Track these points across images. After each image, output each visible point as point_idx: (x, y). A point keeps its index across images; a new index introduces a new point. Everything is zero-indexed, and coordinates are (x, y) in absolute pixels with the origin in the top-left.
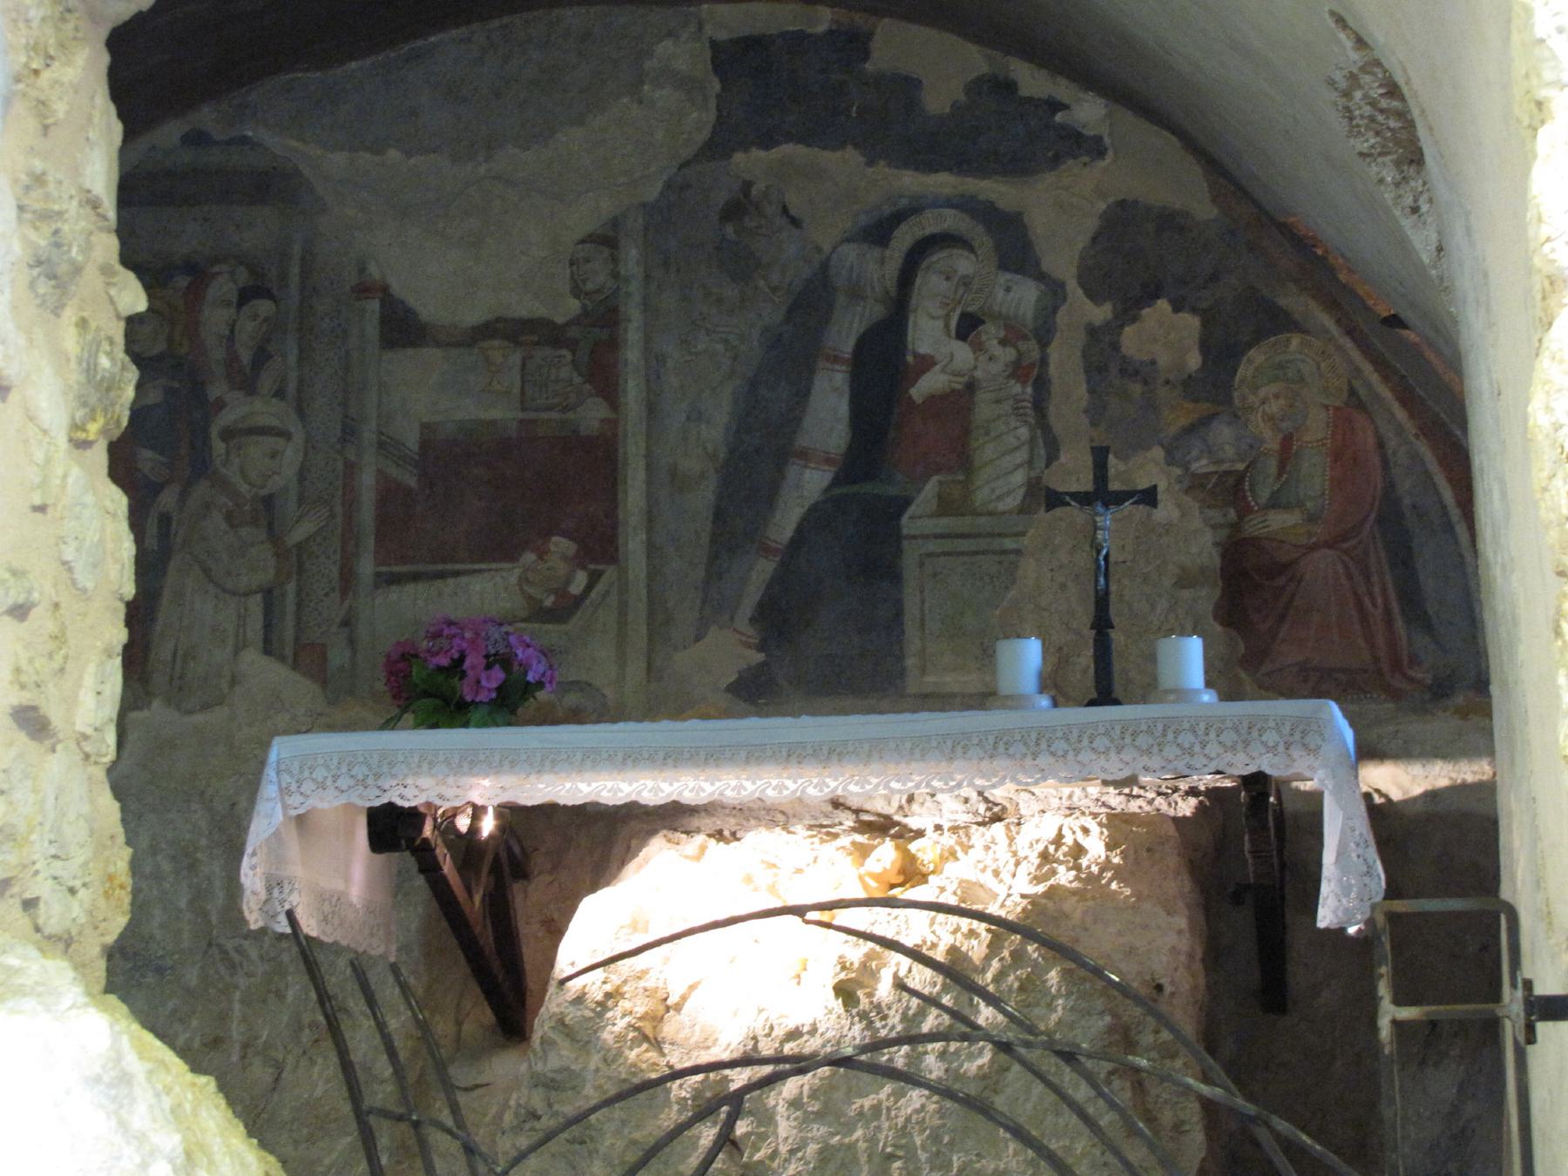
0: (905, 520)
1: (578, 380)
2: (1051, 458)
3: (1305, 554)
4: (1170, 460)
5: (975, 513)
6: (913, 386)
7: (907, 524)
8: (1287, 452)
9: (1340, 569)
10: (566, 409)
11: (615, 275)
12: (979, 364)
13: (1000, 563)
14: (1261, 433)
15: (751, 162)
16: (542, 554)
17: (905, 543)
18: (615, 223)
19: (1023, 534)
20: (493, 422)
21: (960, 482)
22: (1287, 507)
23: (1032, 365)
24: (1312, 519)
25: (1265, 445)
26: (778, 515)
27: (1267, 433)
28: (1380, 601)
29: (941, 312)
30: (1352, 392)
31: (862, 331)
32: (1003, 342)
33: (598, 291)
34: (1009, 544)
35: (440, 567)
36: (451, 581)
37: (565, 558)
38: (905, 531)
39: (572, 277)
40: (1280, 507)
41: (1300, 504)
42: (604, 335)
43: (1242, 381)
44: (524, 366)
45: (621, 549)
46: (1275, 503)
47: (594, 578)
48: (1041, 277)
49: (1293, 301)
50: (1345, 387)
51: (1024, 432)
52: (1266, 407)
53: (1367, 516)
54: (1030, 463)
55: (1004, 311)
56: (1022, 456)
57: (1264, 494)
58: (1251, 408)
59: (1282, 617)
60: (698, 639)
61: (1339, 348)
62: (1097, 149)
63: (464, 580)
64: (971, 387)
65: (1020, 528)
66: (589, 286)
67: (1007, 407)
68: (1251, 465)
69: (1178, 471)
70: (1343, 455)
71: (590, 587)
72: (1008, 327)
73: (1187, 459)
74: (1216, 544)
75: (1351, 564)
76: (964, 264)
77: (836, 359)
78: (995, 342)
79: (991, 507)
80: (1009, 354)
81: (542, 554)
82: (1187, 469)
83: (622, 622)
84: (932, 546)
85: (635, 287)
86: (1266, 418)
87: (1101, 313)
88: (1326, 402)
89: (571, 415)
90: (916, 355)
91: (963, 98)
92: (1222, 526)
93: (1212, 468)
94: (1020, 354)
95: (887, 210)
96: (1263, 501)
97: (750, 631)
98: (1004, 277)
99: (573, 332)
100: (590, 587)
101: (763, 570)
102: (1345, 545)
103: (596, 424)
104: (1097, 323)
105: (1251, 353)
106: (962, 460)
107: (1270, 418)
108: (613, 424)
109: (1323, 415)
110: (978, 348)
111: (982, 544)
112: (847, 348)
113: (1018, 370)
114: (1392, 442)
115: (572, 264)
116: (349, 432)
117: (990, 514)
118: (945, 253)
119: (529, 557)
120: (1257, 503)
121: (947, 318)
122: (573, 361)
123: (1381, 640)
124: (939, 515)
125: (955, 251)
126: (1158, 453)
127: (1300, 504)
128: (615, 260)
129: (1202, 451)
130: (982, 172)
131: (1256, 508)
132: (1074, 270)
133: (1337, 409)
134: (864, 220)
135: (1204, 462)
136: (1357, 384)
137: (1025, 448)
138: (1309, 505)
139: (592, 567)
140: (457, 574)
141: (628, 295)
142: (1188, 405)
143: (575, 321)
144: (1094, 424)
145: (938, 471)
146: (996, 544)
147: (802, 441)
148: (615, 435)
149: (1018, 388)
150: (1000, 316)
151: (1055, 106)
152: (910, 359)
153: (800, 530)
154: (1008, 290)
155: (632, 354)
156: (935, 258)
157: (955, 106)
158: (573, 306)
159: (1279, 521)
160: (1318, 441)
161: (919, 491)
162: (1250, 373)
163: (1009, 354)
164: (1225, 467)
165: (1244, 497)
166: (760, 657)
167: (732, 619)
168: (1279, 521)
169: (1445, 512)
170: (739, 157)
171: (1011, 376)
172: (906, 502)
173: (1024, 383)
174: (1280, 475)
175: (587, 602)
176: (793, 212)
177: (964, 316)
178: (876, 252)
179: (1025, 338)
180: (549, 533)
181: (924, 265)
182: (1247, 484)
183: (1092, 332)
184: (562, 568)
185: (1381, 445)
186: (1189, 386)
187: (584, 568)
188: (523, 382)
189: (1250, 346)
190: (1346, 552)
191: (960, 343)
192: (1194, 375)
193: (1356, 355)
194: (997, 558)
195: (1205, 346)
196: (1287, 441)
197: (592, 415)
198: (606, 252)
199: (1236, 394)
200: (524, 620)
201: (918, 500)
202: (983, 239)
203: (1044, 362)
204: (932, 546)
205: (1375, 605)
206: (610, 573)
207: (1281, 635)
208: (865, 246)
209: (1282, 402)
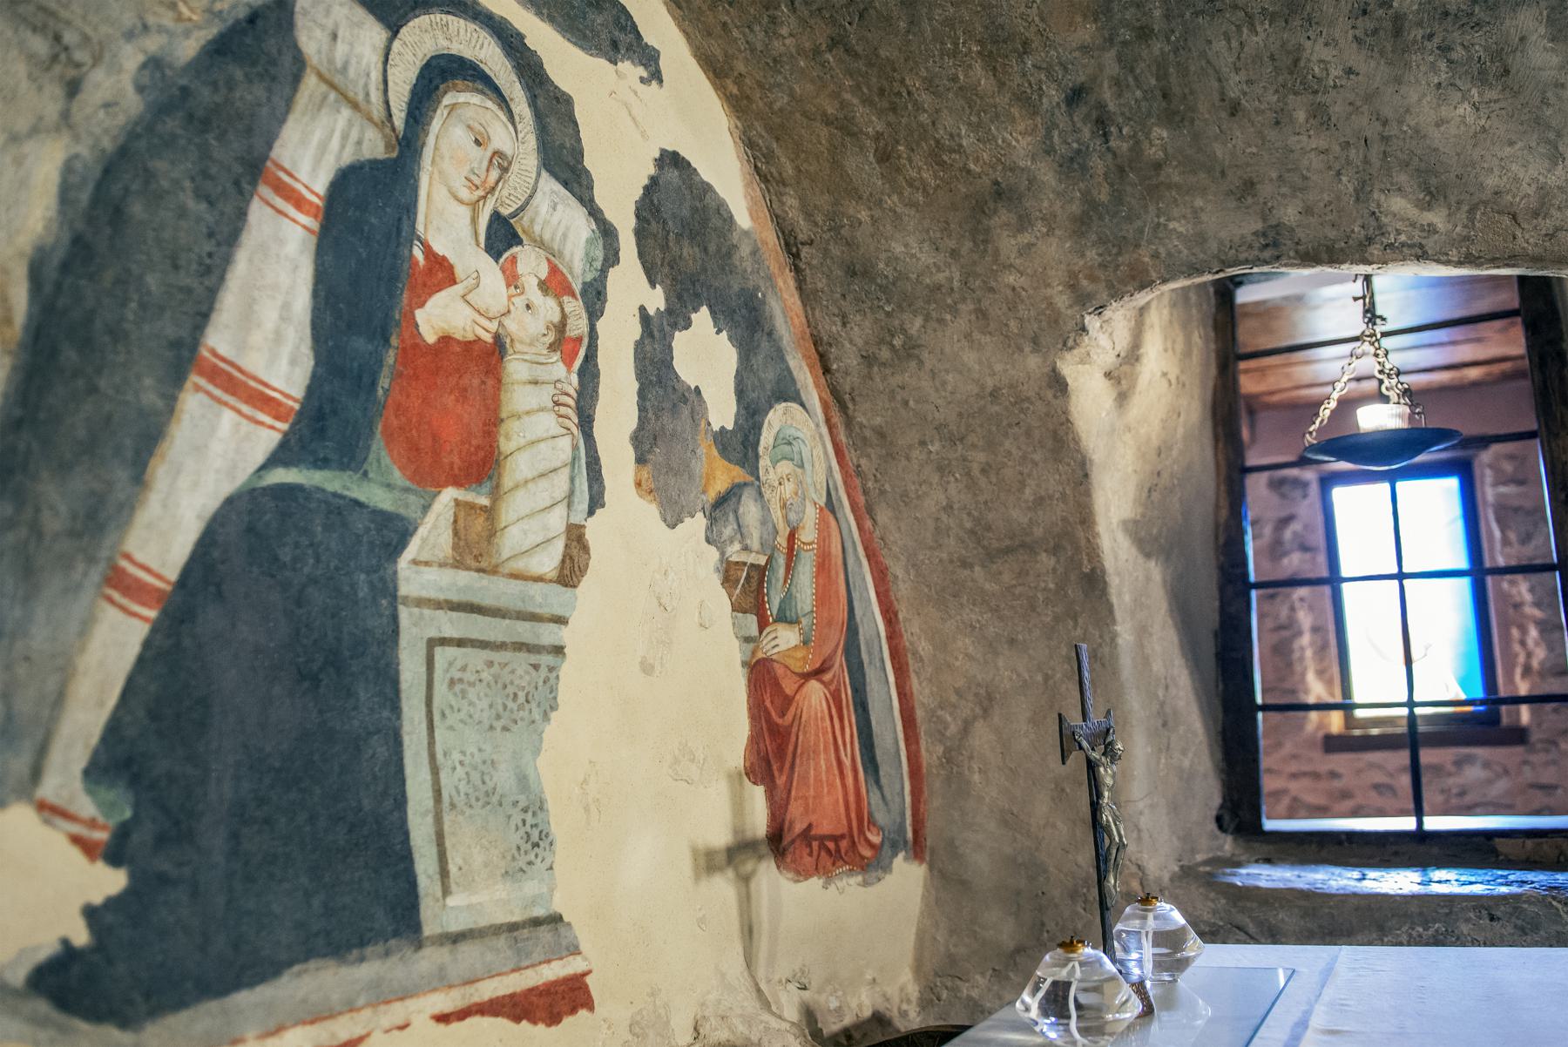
0: (403, 562)
5: (493, 571)
12: (512, 308)
13: (536, 667)
17: (404, 614)
19: (561, 621)
21: (483, 509)
23: (579, 339)
29: (465, 194)
38: (403, 590)
51: (565, 444)
53: (840, 640)
55: (547, 237)
56: (561, 483)
65: (558, 611)
72: (554, 270)
79: (519, 565)
84: (450, 625)
88: (816, 500)
97: (86, 807)
111: (524, 631)
112: (315, 180)
113: (561, 341)
117: (515, 576)
124: (458, 564)
125: (489, 104)
137: (566, 472)
144: (641, 460)
146: (524, 631)
149: (559, 370)
150: (540, 244)
152: (418, 253)
156: (462, 97)
161: (426, 508)
166: (110, 881)
167: (36, 774)
171: (552, 347)
194: (534, 658)
201: (422, 531)
204: (450, 625)
205: (846, 755)
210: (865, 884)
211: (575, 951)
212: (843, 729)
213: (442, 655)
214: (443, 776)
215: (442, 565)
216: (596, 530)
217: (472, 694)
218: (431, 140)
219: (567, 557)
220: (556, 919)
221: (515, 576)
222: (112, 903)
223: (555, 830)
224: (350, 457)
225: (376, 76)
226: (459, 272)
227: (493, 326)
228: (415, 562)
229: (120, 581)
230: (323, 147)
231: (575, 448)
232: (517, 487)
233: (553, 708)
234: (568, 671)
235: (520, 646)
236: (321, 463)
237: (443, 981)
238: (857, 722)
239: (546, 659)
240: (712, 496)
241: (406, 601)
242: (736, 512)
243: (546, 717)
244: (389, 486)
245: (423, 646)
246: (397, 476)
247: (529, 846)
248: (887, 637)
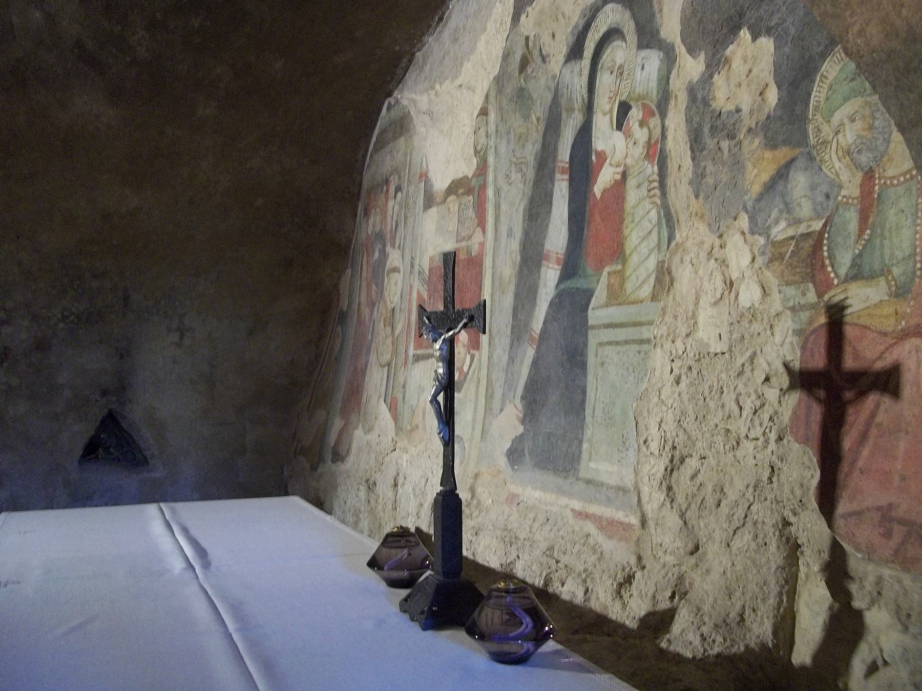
3: (892, 346)
4: (755, 229)
14: (837, 175)
22: (871, 277)
24: (900, 292)
25: (843, 192)
27: (845, 177)
40: (863, 278)
41: (885, 272)
43: (816, 108)
52: (840, 136)
57: (845, 260)
69: (762, 240)
73: (767, 224)
74: (797, 333)
82: (768, 237)
86: (840, 153)
92: (802, 307)
93: (791, 232)
96: (843, 271)
116: (412, 266)
120: (837, 275)
127: (885, 272)
129: (781, 212)
131: (836, 282)
135: (783, 224)
138: (896, 271)
142: (768, 154)
153: (544, 323)
160: (904, 174)
162: (823, 95)
164: (802, 229)
165: (823, 266)
174: (861, 232)
182: (825, 248)
189: (824, 56)
192: (772, 114)
201: (596, 293)
207: (860, 463)
209: (859, 124)
215: (602, 307)
228: (593, 309)
241: (594, 327)
242: (783, 195)
247: (624, 449)
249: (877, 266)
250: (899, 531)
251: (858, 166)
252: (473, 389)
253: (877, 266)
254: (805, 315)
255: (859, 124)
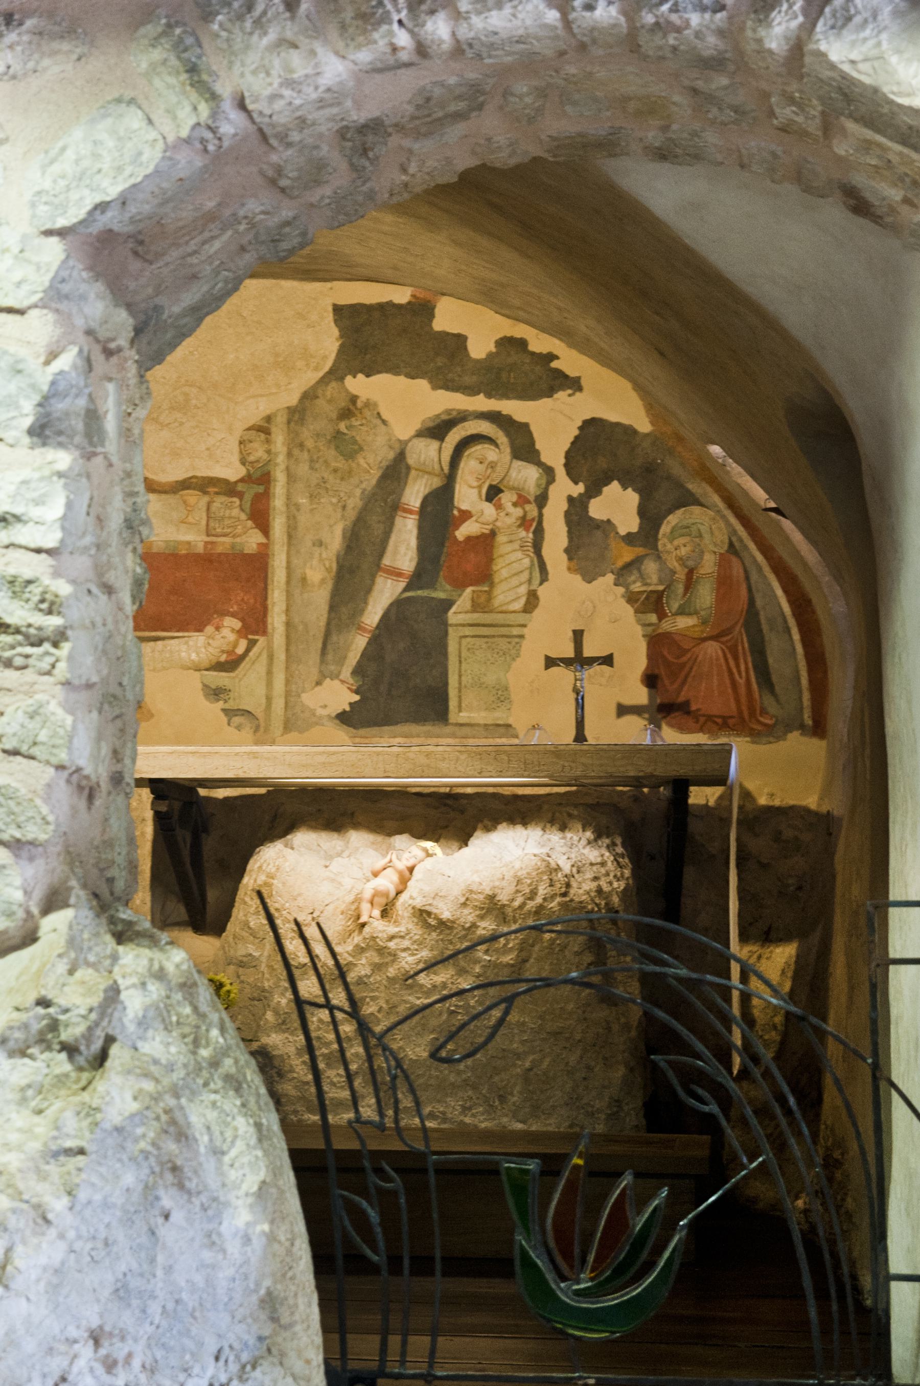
1: (243, 516)
2: (544, 578)
6: (457, 527)
7: (454, 616)
8: (690, 583)
9: (720, 652)
10: (234, 536)
11: (269, 452)
15: (357, 384)
16: (218, 628)
17: (450, 630)
18: (269, 419)
19: (524, 626)
20: (189, 543)
22: (689, 614)
23: (533, 520)
24: (704, 622)
26: (370, 607)
28: (744, 674)
29: (475, 484)
30: (731, 545)
31: (427, 492)
32: (515, 505)
33: (257, 461)
34: (515, 631)
35: (154, 634)
36: (159, 643)
37: (233, 630)
38: (450, 622)
39: (241, 452)
41: (696, 613)
42: (261, 489)
44: (208, 509)
45: (270, 627)
46: (681, 612)
47: (252, 644)
48: (539, 464)
49: (695, 487)
50: (727, 541)
51: (527, 562)
54: (530, 581)
55: (516, 485)
56: (525, 576)
57: (675, 606)
58: (669, 552)
59: (684, 683)
60: (318, 683)
61: (723, 517)
62: (575, 384)
63: (167, 642)
64: (493, 534)
66: (252, 458)
67: (516, 546)
68: (668, 587)
70: (724, 582)
71: (248, 650)
74: (644, 636)
75: (727, 651)
76: (490, 453)
77: (410, 512)
78: (510, 504)
79: (504, 608)
80: (518, 512)
81: (218, 628)
83: (269, 673)
85: (281, 459)
87: (579, 489)
89: (238, 540)
90: (460, 510)
91: (494, 350)
92: (649, 625)
94: (525, 513)
95: (445, 417)
96: (674, 611)
97: (351, 681)
98: (518, 464)
99: (240, 487)
100: (248, 650)
101: (360, 642)
102: (725, 639)
103: (255, 546)
104: (575, 495)
105: (670, 517)
106: (484, 576)
107: (680, 559)
108: (266, 546)
109: (713, 557)
110: (499, 507)
113: (524, 522)
114: (754, 577)
115: (241, 443)
118: (479, 447)
119: (209, 629)
121: (480, 487)
122: (241, 506)
123: (744, 699)
125: (486, 446)
126: (610, 578)
128: (268, 441)
130: (505, 396)
132: (563, 461)
133: (721, 554)
134: (431, 424)
135: (638, 584)
136: (734, 539)
139: (250, 637)
140: (163, 639)
141: (276, 465)
143: (242, 480)
145: (471, 585)
146: (504, 631)
147: (386, 561)
148: (267, 555)
150: (512, 488)
151: (552, 357)
152: (456, 512)
154: (520, 471)
155: (278, 502)
156: (473, 449)
157: (490, 355)
158: (241, 472)
159: (684, 622)
161: (460, 596)
163: (518, 512)
166: (357, 698)
168: (684, 622)
169: (785, 621)
170: (349, 380)
171: (519, 526)
172: (448, 604)
173: (527, 530)
174: (685, 594)
175: (247, 659)
176: (384, 417)
177: (491, 487)
178: (435, 444)
179: (529, 502)
180: (224, 613)
181: (466, 454)
183: (570, 499)
184: (232, 637)
185: (747, 578)
186: (629, 539)
187: (246, 638)
188: (208, 517)
190: (722, 643)
191: (487, 504)
193: (733, 520)
195: (642, 512)
196: (691, 572)
197: (252, 540)
198: (263, 436)
199: (660, 544)
200: (207, 670)
201: (458, 603)
202: (502, 439)
203: (541, 515)
204: (468, 631)
206: (262, 641)
208: (429, 440)
210: (753, 742)
211: (517, 737)
212: (738, 666)
213: (464, 641)
214: (463, 678)
216: (542, 591)
217: (477, 652)
218: (460, 472)
219: (528, 602)
220: (508, 726)
221: (501, 612)
222: (356, 702)
223: (513, 696)
224: (432, 585)
225: (436, 459)
226: (474, 512)
227: (490, 527)
229: (360, 628)
230: (418, 492)
231: (532, 561)
232: (501, 581)
233: (518, 656)
234: (525, 644)
235: (503, 636)
236: (420, 588)
237: (453, 736)
238: (753, 662)
239: (517, 640)
240: (620, 563)
241: (451, 625)
242: (639, 570)
243: (514, 659)
244: (444, 591)
245: (457, 639)
246: (448, 587)
248: (794, 614)
249: (692, 610)
250: (702, 719)
251: (686, 567)
252: (261, 668)
253: (692, 610)
254: (650, 629)
255: (688, 548)
